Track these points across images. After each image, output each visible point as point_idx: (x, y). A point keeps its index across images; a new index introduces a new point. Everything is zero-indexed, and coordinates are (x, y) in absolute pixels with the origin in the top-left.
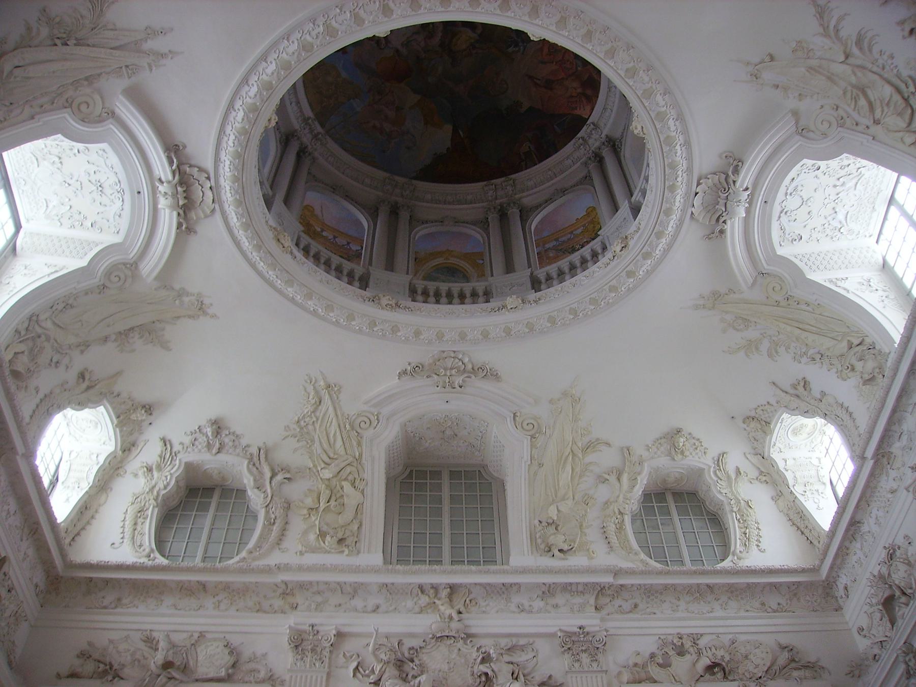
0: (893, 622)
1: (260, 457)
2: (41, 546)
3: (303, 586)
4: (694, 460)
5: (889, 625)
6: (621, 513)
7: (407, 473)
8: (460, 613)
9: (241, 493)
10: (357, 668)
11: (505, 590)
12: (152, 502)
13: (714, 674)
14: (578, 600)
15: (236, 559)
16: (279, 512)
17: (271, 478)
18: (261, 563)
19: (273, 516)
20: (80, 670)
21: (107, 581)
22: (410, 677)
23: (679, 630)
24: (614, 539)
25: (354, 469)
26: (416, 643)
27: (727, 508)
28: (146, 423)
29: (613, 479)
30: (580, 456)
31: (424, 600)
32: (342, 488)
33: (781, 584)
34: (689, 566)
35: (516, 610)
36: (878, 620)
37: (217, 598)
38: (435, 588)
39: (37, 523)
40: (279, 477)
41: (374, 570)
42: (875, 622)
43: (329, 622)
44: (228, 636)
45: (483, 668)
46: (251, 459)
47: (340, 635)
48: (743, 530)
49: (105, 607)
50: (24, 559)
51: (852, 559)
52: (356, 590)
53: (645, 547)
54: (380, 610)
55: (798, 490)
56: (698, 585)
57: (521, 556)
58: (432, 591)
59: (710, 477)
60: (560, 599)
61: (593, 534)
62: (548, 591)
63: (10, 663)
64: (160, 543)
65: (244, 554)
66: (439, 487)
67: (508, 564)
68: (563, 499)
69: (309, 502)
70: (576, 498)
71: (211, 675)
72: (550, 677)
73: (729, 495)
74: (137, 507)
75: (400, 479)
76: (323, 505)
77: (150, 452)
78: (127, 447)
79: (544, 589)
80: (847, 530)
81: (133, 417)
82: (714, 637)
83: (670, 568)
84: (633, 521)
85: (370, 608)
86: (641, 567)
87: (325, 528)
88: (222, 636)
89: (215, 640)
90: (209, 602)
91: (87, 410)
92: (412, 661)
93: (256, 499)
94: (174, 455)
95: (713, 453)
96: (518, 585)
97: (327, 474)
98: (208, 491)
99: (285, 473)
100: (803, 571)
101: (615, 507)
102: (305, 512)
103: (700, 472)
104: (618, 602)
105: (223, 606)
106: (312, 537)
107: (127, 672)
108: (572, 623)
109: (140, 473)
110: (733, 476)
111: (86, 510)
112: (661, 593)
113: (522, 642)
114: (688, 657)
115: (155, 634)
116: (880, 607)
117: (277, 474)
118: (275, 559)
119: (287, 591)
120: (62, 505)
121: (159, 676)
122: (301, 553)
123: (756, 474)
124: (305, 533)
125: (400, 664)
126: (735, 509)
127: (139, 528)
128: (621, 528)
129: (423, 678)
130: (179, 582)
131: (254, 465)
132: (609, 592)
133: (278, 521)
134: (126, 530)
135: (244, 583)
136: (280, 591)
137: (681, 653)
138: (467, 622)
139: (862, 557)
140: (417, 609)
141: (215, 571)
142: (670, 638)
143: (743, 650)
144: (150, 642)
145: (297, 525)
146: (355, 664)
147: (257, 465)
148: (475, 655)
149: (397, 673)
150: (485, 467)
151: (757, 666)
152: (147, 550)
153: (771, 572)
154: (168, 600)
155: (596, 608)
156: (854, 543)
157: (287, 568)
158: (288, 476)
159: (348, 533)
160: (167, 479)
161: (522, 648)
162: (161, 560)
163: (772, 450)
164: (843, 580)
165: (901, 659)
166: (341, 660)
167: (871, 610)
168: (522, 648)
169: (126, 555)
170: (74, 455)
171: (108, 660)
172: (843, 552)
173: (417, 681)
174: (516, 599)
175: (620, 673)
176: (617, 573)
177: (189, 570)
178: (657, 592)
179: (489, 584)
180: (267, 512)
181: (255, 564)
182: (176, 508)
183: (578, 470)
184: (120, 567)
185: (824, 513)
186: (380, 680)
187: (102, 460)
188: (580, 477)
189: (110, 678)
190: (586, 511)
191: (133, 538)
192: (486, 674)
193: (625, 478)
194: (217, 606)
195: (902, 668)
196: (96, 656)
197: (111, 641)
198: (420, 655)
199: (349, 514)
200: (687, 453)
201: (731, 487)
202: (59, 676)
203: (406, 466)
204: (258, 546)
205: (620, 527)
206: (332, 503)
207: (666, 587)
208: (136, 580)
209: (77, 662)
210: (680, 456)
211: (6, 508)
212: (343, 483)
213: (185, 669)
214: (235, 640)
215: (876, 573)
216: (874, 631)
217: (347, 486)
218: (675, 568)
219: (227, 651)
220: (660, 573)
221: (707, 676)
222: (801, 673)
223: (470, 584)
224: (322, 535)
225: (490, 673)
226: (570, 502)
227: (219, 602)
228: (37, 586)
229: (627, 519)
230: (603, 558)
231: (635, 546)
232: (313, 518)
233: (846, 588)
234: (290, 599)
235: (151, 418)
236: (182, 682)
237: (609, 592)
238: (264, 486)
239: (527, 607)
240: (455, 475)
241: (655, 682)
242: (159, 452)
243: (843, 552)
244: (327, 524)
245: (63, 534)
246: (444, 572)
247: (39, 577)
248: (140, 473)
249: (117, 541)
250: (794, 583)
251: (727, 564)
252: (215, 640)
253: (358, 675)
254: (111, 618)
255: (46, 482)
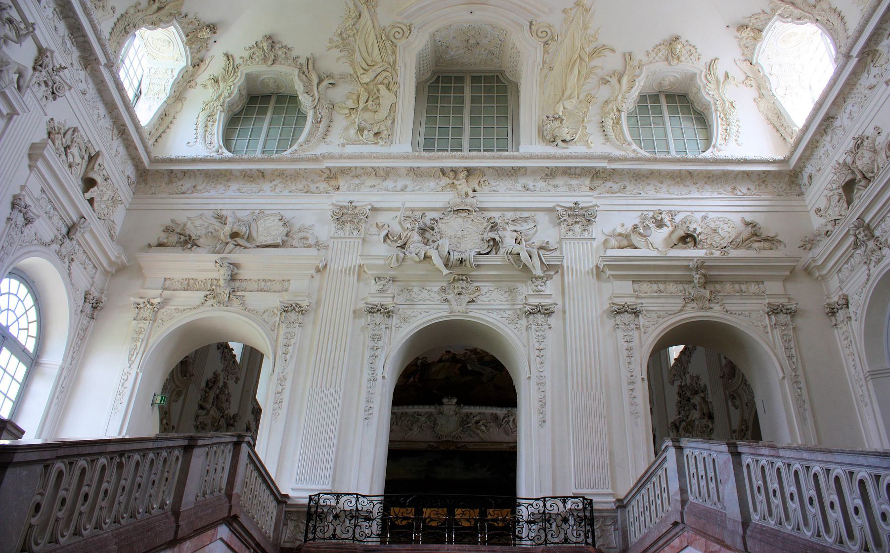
0: (849, 203)
1: (307, 67)
2: (129, 145)
3: (344, 171)
4: (687, 66)
5: (845, 205)
6: (619, 111)
7: (434, 78)
8: (474, 191)
9: (294, 98)
10: (387, 235)
11: (514, 173)
12: (219, 108)
13: (686, 243)
14: (574, 182)
15: (289, 151)
16: (325, 112)
17: (318, 84)
18: (309, 153)
19: (320, 116)
20: (165, 241)
21: (184, 172)
22: (430, 241)
23: (659, 208)
24: (610, 132)
25: (388, 74)
26: (436, 215)
27: (713, 108)
28: (211, 42)
29: (614, 81)
30: (587, 60)
31: (445, 181)
32: (378, 90)
33: (752, 172)
34: (673, 154)
35: (522, 189)
36: (836, 201)
37: (274, 183)
38: (454, 171)
39: (124, 125)
40: (325, 83)
41: (406, 157)
42: (832, 204)
43: (364, 197)
44: (282, 212)
45: (492, 235)
46: (300, 69)
47: (374, 209)
48: (725, 127)
49: (183, 193)
50: (116, 155)
51: (821, 151)
52: (388, 173)
53: (638, 140)
54: (408, 189)
55: (779, 93)
56: (680, 171)
57: (530, 147)
58: (452, 174)
59: (701, 81)
60: (560, 181)
61: (592, 128)
62: (550, 174)
63: (111, 237)
64: (227, 142)
65: (295, 147)
66: (462, 90)
67: (517, 150)
68: (570, 98)
69: (350, 104)
70: (580, 97)
71: (268, 242)
72: (547, 243)
73: (716, 97)
74: (207, 112)
75: (428, 84)
76: (362, 105)
77: (215, 65)
78: (197, 63)
79: (548, 172)
80: (820, 125)
81: (200, 35)
82: (689, 214)
83: (657, 156)
84: (629, 118)
85: (399, 188)
86: (632, 155)
87: (363, 124)
88: (277, 212)
89: (271, 215)
90: (267, 186)
91: (159, 30)
92: (433, 229)
93: (305, 100)
94: (236, 68)
95: (706, 59)
96: (525, 168)
97: (366, 79)
98: (266, 98)
99: (328, 80)
100: (775, 162)
101: (613, 105)
102: (347, 111)
103: (693, 77)
104: (609, 184)
105: (278, 190)
106: (352, 132)
107: (201, 241)
108: (568, 201)
109: (209, 84)
110: (722, 79)
111: (165, 117)
112: (647, 178)
113: (526, 214)
114: (665, 228)
115: (224, 213)
116: (840, 191)
117: (323, 80)
118: (321, 149)
119: (331, 175)
120: (145, 113)
121: (227, 243)
122: (343, 146)
123: (743, 77)
124: (347, 129)
125: (423, 231)
126: (719, 109)
127: (209, 129)
128: (618, 123)
129: (440, 242)
130: (241, 171)
131: (303, 73)
132: (603, 175)
133: (324, 120)
134: (199, 131)
135: (295, 170)
136: (325, 175)
137: (660, 224)
138: (480, 199)
139: (830, 149)
140: (440, 189)
141: (272, 160)
142: (651, 214)
143: (713, 225)
144: (221, 219)
145: (340, 121)
146: (385, 232)
147: (306, 73)
148: (485, 224)
149: (420, 239)
150: (502, 72)
151: (723, 238)
152: (217, 146)
153: (746, 162)
154: (234, 186)
155: (591, 189)
156: (824, 137)
157: (331, 157)
158: (332, 81)
159: (383, 127)
160: (233, 88)
161: (525, 220)
162: (227, 154)
163: (760, 56)
164: (809, 169)
165: (851, 232)
166: (374, 230)
167: (832, 193)
168: (525, 220)
169: (199, 150)
170: (153, 71)
171: (187, 233)
172: (813, 145)
173: (436, 244)
174: (522, 181)
175: (606, 241)
176: (610, 159)
177: (249, 160)
178: (643, 176)
179: (500, 168)
180: (315, 113)
181: (303, 155)
182: (240, 113)
183: (584, 72)
184: (194, 161)
185: (799, 110)
186: (405, 244)
187: (176, 74)
188: (586, 79)
189: (189, 246)
190: (588, 109)
191: (205, 138)
192: (494, 240)
193: (625, 80)
194: (273, 189)
195: (852, 239)
196: (178, 230)
197: (189, 218)
198: (440, 225)
199: (383, 113)
200: (682, 59)
201: (718, 89)
202: (150, 246)
203: (434, 73)
204: (307, 141)
205: (617, 122)
206: (370, 103)
207: (652, 173)
208: (208, 170)
209: (164, 235)
210: (676, 61)
211: (96, 112)
212: (380, 87)
213: (249, 238)
214: (288, 215)
215: (841, 161)
216: (830, 212)
217: (382, 88)
218: (662, 156)
219: (281, 223)
220: (648, 160)
221: (680, 245)
222: (761, 244)
223: (485, 167)
224: (361, 130)
225: (498, 239)
226: (574, 101)
227: (276, 185)
228: (129, 178)
229: (624, 116)
230: (598, 146)
231: (629, 138)
232: (354, 117)
233: (810, 177)
234: (333, 183)
235: (215, 37)
236: (245, 248)
237: (603, 175)
238: (312, 91)
239: (531, 187)
240: (475, 79)
241: (636, 248)
242: (223, 66)
243: (813, 145)
244: (365, 120)
245: (146, 136)
246: (463, 158)
247: (130, 170)
248: (209, 84)
249: (193, 139)
250: (764, 172)
251: (708, 154)
252: (271, 215)
253: (388, 240)
254: (189, 201)
255: (131, 95)
